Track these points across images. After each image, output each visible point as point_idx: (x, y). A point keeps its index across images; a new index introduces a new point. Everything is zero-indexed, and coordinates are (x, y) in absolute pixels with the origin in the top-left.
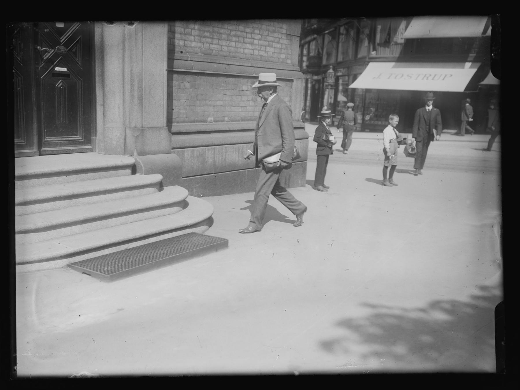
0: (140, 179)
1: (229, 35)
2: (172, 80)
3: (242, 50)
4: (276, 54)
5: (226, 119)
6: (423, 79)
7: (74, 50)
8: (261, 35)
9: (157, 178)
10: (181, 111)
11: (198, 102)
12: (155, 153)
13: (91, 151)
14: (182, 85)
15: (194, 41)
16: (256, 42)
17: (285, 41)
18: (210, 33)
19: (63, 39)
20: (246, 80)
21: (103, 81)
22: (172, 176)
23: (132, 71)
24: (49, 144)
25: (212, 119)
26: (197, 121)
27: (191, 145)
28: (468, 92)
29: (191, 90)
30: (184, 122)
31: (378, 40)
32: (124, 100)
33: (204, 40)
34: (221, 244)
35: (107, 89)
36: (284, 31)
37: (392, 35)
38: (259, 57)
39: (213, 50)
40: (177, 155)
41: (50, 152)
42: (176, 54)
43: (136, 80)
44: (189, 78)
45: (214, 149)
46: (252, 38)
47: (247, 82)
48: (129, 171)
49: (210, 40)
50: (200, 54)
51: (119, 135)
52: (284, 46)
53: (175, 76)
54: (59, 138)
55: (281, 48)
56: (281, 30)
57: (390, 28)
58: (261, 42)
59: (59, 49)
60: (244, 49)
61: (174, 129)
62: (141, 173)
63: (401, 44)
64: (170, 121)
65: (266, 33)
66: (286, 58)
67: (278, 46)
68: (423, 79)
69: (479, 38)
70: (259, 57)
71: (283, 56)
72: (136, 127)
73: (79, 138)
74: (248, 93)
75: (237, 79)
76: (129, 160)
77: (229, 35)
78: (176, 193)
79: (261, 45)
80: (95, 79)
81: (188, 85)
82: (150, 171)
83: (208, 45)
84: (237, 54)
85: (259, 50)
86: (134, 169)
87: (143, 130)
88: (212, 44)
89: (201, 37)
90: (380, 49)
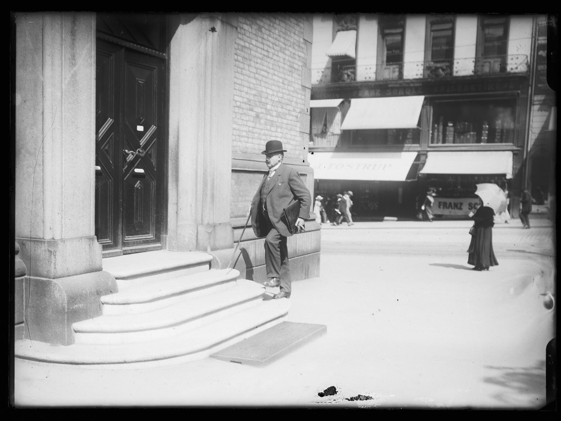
1: (260, 134)
7: (150, 153)
11: (240, 198)
12: (223, 248)
17: (299, 139)
18: (247, 132)
19: (142, 142)
21: (177, 180)
28: (409, 181)
29: (235, 186)
33: (242, 139)
35: (180, 188)
36: (298, 129)
43: (209, 179)
48: (208, 266)
49: (246, 139)
50: (239, 152)
57: (326, 118)
59: (139, 152)
62: (218, 268)
66: (300, 154)
69: (413, 129)
71: (297, 152)
72: (208, 224)
73: (150, 236)
77: (260, 134)
87: (214, 226)
90: (315, 138)
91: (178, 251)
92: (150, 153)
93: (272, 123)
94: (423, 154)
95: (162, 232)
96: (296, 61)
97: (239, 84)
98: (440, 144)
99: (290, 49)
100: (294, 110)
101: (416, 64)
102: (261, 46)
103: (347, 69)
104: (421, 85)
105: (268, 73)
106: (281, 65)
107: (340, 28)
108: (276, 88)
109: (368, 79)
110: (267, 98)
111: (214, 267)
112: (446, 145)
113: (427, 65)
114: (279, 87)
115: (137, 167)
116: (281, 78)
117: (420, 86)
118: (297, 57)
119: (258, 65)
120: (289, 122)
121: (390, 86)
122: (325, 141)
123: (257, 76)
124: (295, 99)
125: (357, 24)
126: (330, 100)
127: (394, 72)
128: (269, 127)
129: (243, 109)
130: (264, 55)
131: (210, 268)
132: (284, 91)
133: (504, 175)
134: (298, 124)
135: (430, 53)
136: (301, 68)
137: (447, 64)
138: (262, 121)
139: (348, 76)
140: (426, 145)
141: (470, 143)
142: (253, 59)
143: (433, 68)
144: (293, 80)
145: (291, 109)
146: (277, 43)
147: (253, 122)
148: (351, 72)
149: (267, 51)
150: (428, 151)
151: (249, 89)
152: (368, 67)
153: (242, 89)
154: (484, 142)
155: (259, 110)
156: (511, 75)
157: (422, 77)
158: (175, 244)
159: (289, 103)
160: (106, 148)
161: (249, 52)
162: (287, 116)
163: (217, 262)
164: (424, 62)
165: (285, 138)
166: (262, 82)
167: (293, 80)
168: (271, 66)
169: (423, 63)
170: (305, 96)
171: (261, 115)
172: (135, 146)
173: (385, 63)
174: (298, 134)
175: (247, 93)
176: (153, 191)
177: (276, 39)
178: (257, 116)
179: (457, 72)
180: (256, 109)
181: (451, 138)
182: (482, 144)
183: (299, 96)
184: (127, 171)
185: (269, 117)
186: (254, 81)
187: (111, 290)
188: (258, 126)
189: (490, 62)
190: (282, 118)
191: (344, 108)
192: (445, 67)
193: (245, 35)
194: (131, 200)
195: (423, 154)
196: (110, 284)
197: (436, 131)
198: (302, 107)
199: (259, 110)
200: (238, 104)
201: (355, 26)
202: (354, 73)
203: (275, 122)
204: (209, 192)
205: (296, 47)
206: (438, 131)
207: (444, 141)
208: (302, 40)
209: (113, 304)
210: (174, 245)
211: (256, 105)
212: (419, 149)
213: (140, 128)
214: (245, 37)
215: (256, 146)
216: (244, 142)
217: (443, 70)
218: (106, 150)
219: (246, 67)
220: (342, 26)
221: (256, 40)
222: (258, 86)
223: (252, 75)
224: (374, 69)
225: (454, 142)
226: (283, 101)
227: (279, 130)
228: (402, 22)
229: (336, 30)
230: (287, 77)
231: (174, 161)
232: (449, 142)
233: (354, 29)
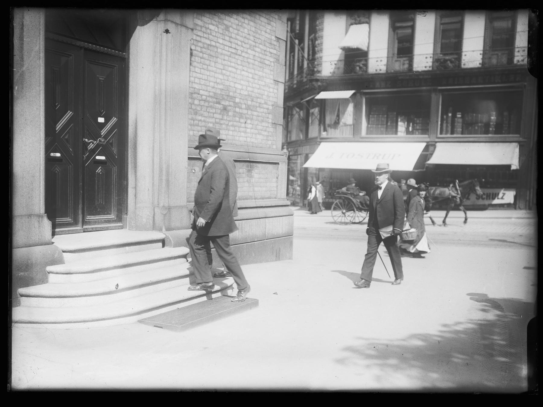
1: (228, 125)
3: (238, 138)
6: (373, 158)
7: (111, 141)
8: (253, 125)
12: (179, 229)
13: (122, 228)
16: (248, 130)
17: (271, 130)
19: (103, 132)
21: (135, 167)
23: (161, 158)
24: (89, 222)
28: (416, 171)
32: (153, 183)
35: (138, 174)
36: (270, 121)
37: (341, 116)
38: (251, 144)
41: (91, 230)
43: (164, 167)
47: (243, 166)
48: (160, 244)
51: (148, 213)
52: (270, 134)
54: (97, 217)
55: (268, 136)
56: (268, 119)
58: (253, 131)
59: (100, 141)
62: (170, 246)
63: (350, 125)
65: (256, 123)
67: (266, 133)
68: (373, 158)
70: (251, 144)
71: (270, 142)
72: (164, 206)
73: (112, 216)
74: (244, 175)
77: (228, 125)
80: (127, 166)
84: (234, 142)
86: (163, 242)
87: (169, 208)
90: (329, 130)
91: (136, 230)
92: (111, 141)
93: (241, 115)
94: (432, 145)
95: (123, 213)
96: (267, 58)
97: (205, 80)
98: (449, 135)
99: (261, 46)
100: (266, 103)
101: (425, 56)
102: (229, 44)
103: (360, 61)
104: (430, 77)
105: (237, 69)
106: (251, 61)
107: (353, 21)
108: (246, 83)
109: (378, 72)
112: (455, 135)
113: (436, 58)
114: (248, 82)
115: (99, 155)
116: (251, 73)
118: (268, 53)
119: (226, 62)
120: (260, 114)
121: (400, 78)
122: (338, 131)
123: (224, 72)
124: (266, 93)
125: (369, 18)
126: (335, 92)
127: (404, 64)
128: (237, 119)
129: (209, 102)
130: (232, 52)
131: (163, 246)
132: (254, 85)
133: (509, 166)
134: (270, 116)
135: (439, 45)
136: (272, 64)
137: (456, 56)
138: (230, 113)
139: (360, 68)
140: (435, 135)
141: (478, 134)
142: (220, 56)
143: (442, 61)
144: (264, 74)
145: (263, 102)
146: (246, 41)
147: (220, 114)
148: (363, 64)
149: (235, 49)
150: (436, 142)
151: (215, 84)
152: (379, 60)
153: (208, 84)
154: (492, 134)
155: (227, 103)
156: (518, 67)
157: (431, 69)
160: (66, 137)
161: (216, 50)
162: (258, 108)
163: (170, 240)
164: (433, 54)
165: (256, 129)
166: (230, 78)
167: (264, 74)
168: (239, 62)
169: (432, 56)
170: (277, 90)
172: (95, 136)
173: (396, 55)
174: (270, 125)
175: (213, 87)
176: (114, 176)
177: (245, 37)
178: (225, 109)
179: (464, 65)
180: (223, 103)
181: (460, 130)
182: (490, 135)
183: (271, 90)
184: (88, 158)
185: (237, 110)
186: (221, 77)
187: (59, 261)
188: (225, 117)
189: (497, 54)
190: (251, 110)
192: (453, 60)
193: (211, 34)
194: (89, 185)
195: (432, 145)
196: (56, 256)
197: (445, 122)
198: (275, 100)
200: (204, 97)
201: (367, 20)
202: (366, 65)
203: (245, 114)
204: (164, 178)
205: (268, 45)
206: (447, 123)
207: (452, 133)
208: (274, 38)
209: (57, 273)
210: (133, 224)
211: (223, 99)
212: (428, 140)
213: (101, 120)
214: (211, 37)
217: (451, 62)
218: (67, 140)
219: (213, 64)
220: (355, 20)
221: (223, 39)
222: (226, 82)
223: (219, 71)
224: (385, 61)
225: (462, 133)
226: (253, 95)
228: (412, 16)
229: (350, 24)
230: (257, 72)
231: (133, 150)
232: (457, 134)
233: (367, 23)
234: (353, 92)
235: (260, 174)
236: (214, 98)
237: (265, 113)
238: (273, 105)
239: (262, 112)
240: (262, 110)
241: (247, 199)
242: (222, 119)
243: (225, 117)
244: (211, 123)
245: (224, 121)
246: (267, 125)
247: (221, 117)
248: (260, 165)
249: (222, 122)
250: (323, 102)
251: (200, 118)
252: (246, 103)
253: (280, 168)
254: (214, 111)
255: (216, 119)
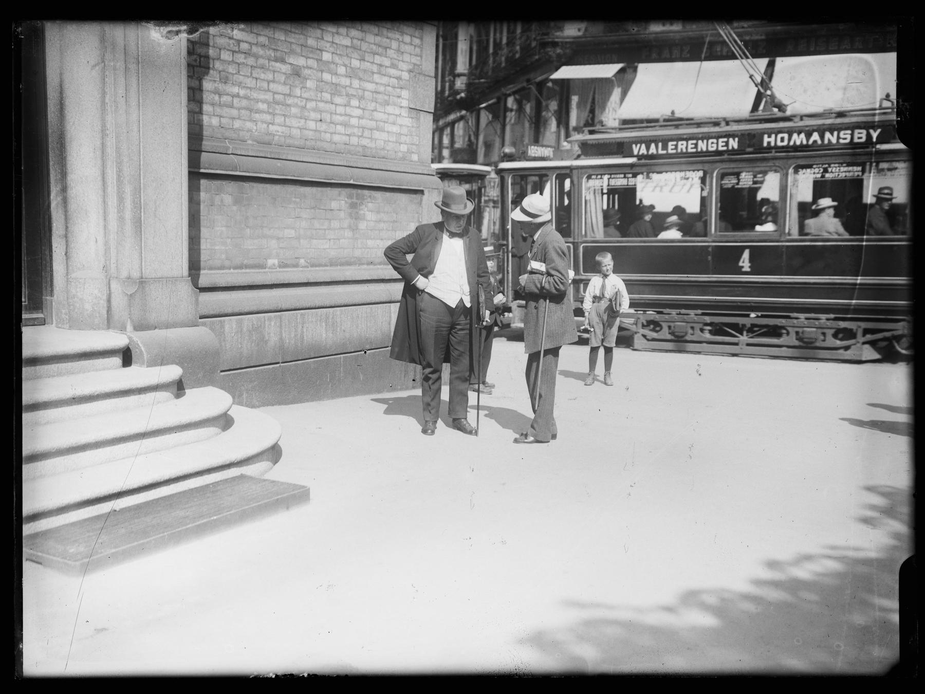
0: (138, 375)
1: (304, 108)
2: (198, 190)
3: (328, 135)
4: (390, 144)
5: (302, 261)
6: (653, 190)
8: (363, 109)
9: (173, 372)
10: (217, 248)
11: (248, 231)
12: (168, 326)
14: (217, 199)
15: (239, 118)
17: (407, 122)
18: (269, 103)
20: (336, 191)
22: (199, 369)
25: (276, 262)
26: (247, 267)
27: (237, 310)
29: (235, 208)
30: (222, 268)
31: (573, 122)
32: (105, 227)
33: (257, 116)
34: (296, 496)
35: (72, 206)
36: (405, 103)
38: (361, 149)
39: (274, 135)
40: (211, 329)
42: (204, 143)
44: (230, 186)
45: (280, 317)
46: (346, 115)
47: (339, 195)
48: (117, 360)
49: (268, 117)
50: (250, 142)
51: (96, 291)
53: (203, 182)
56: (399, 100)
57: (594, 99)
60: (332, 133)
61: (204, 281)
64: (194, 266)
65: (372, 106)
67: (395, 129)
70: (361, 149)
71: (404, 148)
72: (129, 278)
74: (342, 214)
75: (319, 189)
76: (118, 340)
77: (304, 108)
78: (208, 400)
79: (363, 128)
81: (228, 199)
82: (160, 360)
83: (265, 126)
84: (319, 144)
85: (359, 137)
86: (127, 357)
87: (142, 282)
88: (273, 124)
89: (251, 110)
91: (71, 328)
93: (336, 89)
95: (44, 292)
100: (393, 66)
104: (763, 37)
110: (323, 39)
111: (136, 363)
117: (762, 40)
120: (382, 89)
128: (327, 96)
129: (257, 57)
134: (405, 93)
138: (309, 84)
145: (387, 62)
147: (285, 84)
155: (301, 62)
158: (66, 314)
159: (380, 50)
171: (307, 72)
174: (404, 113)
180: (291, 60)
185: (327, 77)
188: (298, 92)
190: (360, 79)
191: (625, 79)
199: (301, 62)
210: (63, 316)
211: (292, 52)
215: (296, 132)
216: (263, 122)
227: (355, 102)
234: (619, 66)
235: (378, 212)
236: (270, 49)
237: (394, 87)
238: (410, 71)
239: (386, 85)
240: (385, 80)
241: (349, 264)
242: (289, 95)
243: (298, 92)
244: (263, 101)
245: (296, 100)
246: (397, 112)
247: (288, 92)
248: (378, 195)
249: (290, 101)
250: (565, 85)
251: (235, 90)
252: (347, 62)
253: (424, 202)
254: (270, 76)
255: (275, 93)
